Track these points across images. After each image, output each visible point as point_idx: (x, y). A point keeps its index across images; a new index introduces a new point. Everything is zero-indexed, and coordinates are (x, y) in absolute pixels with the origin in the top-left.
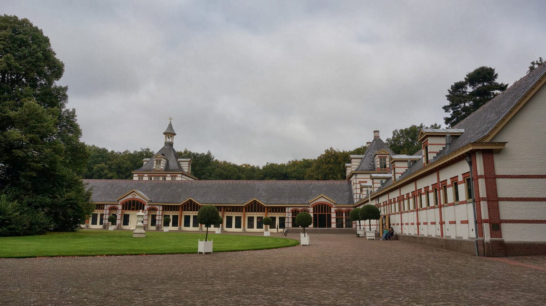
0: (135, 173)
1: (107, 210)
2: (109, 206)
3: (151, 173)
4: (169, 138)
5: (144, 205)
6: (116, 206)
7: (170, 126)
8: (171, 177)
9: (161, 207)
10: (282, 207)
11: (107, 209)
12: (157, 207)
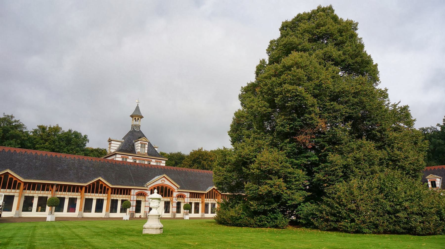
0: (118, 154)
1: (135, 195)
2: (137, 191)
3: (136, 156)
4: (136, 121)
5: (172, 192)
6: (145, 191)
7: (137, 109)
8: (155, 162)
9: (189, 193)
10: (127, 189)
11: (135, 194)
12: (185, 194)
